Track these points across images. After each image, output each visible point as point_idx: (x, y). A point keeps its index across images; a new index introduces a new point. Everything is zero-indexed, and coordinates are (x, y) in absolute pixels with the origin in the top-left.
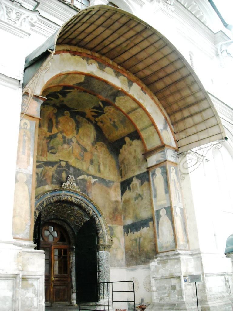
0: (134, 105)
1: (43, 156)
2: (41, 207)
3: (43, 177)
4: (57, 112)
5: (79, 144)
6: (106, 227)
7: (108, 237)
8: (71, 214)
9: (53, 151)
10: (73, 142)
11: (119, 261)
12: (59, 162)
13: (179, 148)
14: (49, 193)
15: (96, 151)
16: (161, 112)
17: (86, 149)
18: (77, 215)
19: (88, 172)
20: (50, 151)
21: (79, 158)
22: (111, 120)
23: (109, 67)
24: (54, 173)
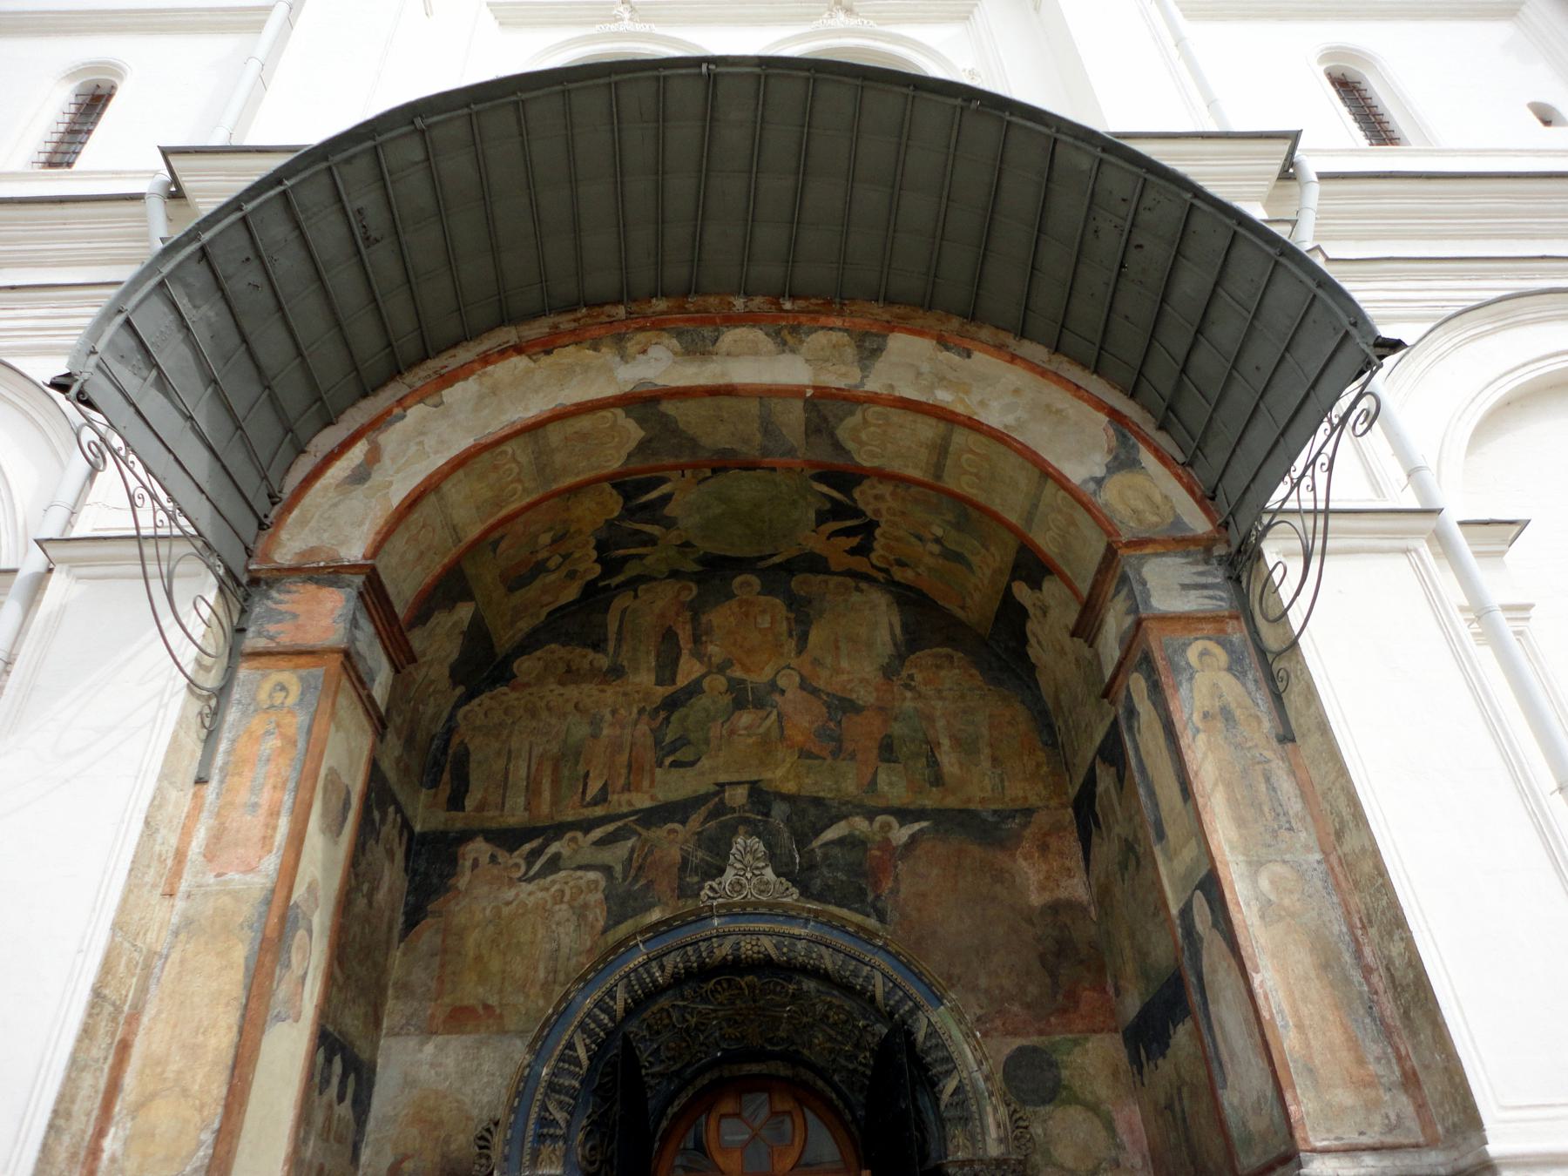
0: (927, 430)
1: (638, 789)
2: (602, 1016)
3: (636, 879)
4: (699, 595)
5: (815, 692)
6: (979, 1054)
7: (995, 1109)
8: (805, 1020)
10: (783, 692)
12: (716, 794)
13: (1226, 525)
14: (644, 942)
15: (909, 694)
16: (1080, 398)
17: (851, 701)
18: (831, 1020)
19: (870, 802)
20: (668, 761)
21: (815, 750)
22: (920, 538)
23: (736, 327)
24: (690, 847)
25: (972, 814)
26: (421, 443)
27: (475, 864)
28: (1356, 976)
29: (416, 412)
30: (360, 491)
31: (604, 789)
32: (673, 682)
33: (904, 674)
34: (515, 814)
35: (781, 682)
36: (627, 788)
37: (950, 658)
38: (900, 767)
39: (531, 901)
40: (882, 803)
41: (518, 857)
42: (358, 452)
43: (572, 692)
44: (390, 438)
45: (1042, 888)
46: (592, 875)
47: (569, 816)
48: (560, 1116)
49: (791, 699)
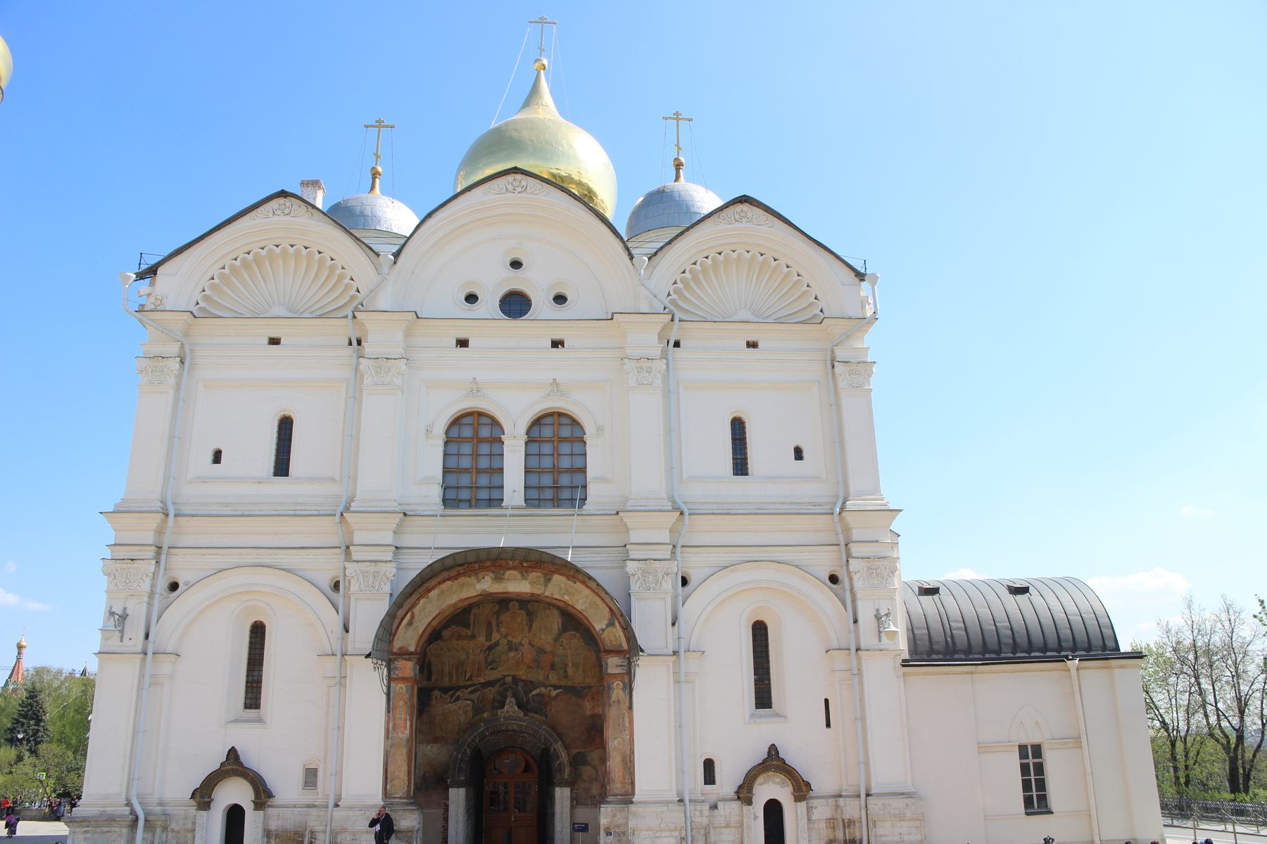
5: (533, 646)
9: (494, 665)
11: (594, 797)
15: (561, 648)
20: (489, 668)
25: (575, 688)
26: (424, 612)
27: (436, 698)
28: (629, 762)
29: (422, 601)
31: (471, 676)
32: (490, 641)
33: (560, 640)
34: (446, 683)
35: (523, 642)
36: (477, 676)
37: (575, 635)
38: (555, 672)
39: (452, 709)
41: (447, 696)
43: (460, 643)
44: (416, 610)
45: (590, 709)
46: (468, 702)
47: (462, 683)
48: (464, 766)
49: (526, 648)
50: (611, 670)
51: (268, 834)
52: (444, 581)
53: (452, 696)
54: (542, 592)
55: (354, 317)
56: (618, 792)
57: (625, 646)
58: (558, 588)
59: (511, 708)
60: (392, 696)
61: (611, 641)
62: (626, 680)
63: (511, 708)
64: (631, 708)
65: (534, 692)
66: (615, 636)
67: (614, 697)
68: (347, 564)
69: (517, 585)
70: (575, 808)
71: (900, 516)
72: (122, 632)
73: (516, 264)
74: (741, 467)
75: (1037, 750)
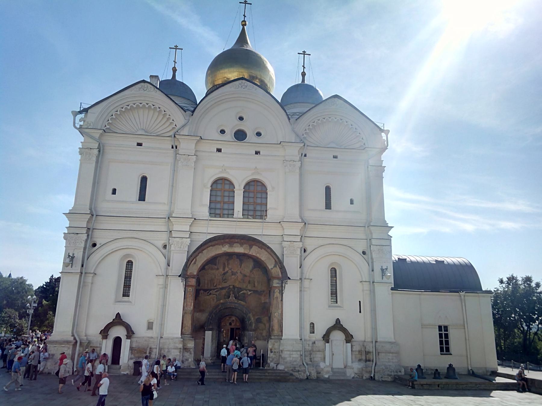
15: (253, 275)
19: (247, 289)
27: (202, 294)
29: (200, 254)
30: (195, 265)
31: (216, 285)
34: (206, 288)
36: (219, 285)
40: (248, 289)
42: (195, 259)
44: (197, 258)
46: (215, 296)
47: (212, 288)
49: (239, 274)
50: (275, 285)
51: (131, 349)
52: (209, 247)
53: (209, 292)
54: (248, 252)
55: (175, 137)
56: (275, 335)
57: (280, 275)
58: (254, 251)
59: (232, 298)
60: (186, 292)
61: (275, 273)
62: (280, 289)
63: (232, 298)
64: (282, 300)
65: (241, 292)
66: (276, 271)
67: (275, 296)
68: (170, 238)
69: (239, 249)
70: (256, 341)
71: (393, 229)
72: (72, 264)
73: (241, 119)
74: (328, 206)
75: (446, 329)
